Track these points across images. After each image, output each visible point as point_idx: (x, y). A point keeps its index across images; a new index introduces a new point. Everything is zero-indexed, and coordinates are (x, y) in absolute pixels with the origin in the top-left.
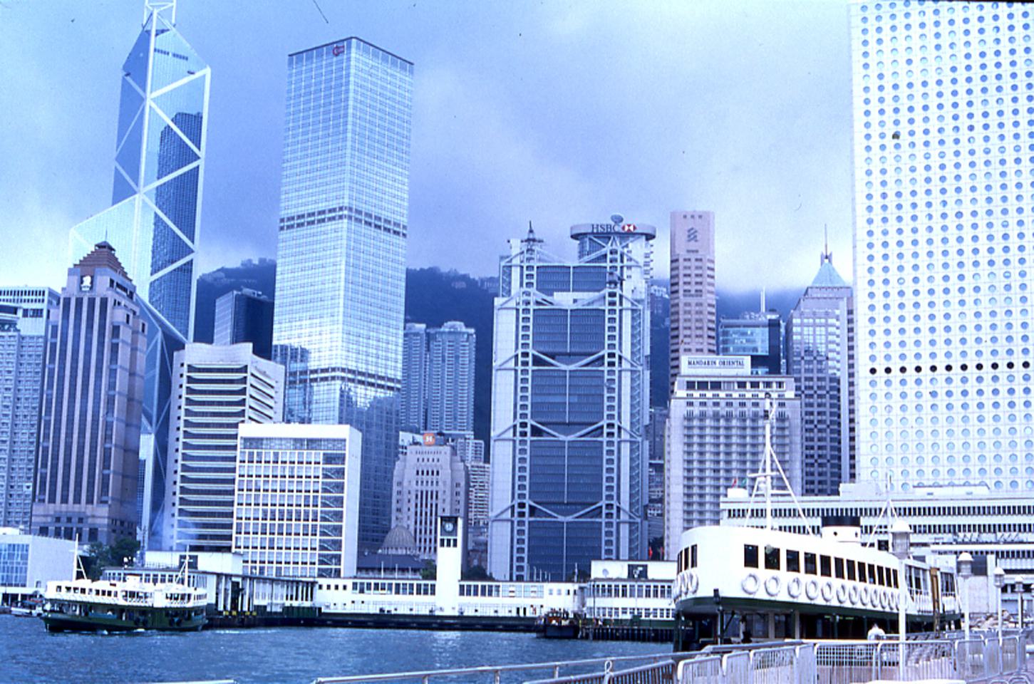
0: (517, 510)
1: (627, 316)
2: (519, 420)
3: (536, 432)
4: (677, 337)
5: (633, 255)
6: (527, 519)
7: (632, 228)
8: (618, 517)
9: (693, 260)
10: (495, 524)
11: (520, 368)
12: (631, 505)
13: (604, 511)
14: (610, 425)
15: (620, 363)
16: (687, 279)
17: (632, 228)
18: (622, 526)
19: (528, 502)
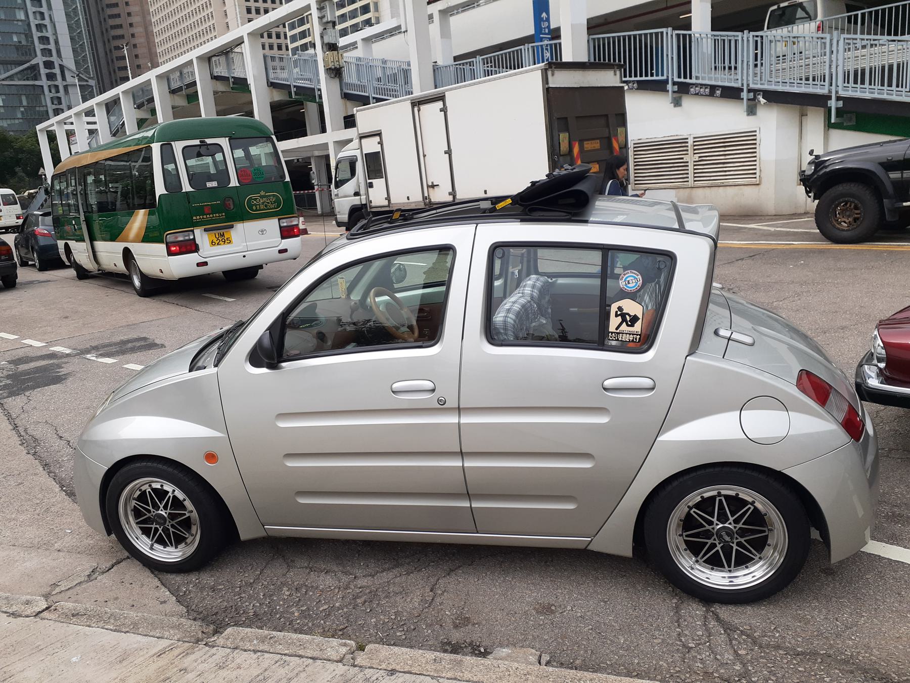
8: (64, 78)
12: (76, 62)
13: (43, 71)
18: (70, 90)
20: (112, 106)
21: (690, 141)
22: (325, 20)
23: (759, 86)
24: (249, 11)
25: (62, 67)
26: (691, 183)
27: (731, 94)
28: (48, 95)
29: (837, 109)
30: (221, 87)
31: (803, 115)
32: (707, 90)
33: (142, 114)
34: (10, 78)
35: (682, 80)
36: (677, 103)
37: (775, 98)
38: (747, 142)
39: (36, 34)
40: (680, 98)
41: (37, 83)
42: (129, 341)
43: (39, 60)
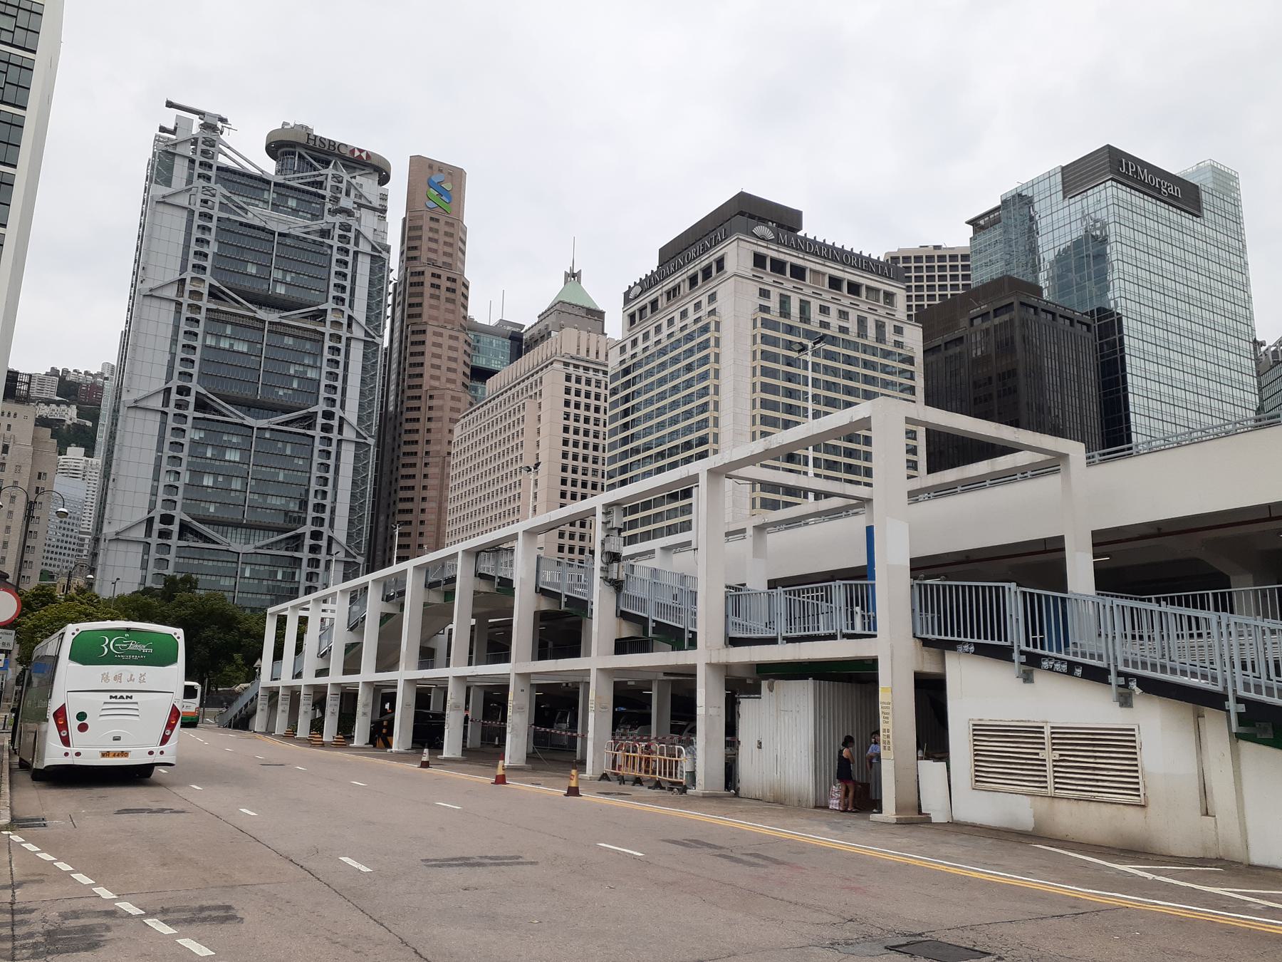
0: (157, 526)
1: (364, 265)
2: (175, 383)
3: (201, 405)
4: (420, 315)
5: (364, 191)
6: (174, 541)
7: (364, 155)
9: (442, 222)
10: (113, 546)
11: (186, 300)
12: (349, 536)
13: (308, 542)
14: (328, 415)
15: (349, 326)
16: (434, 246)
17: (364, 155)
19: (179, 514)
20: (357, 596)
21: (1047, 731)
22: (609, 526)
23: (1130, 670)
24: (563, 495)
25: (330, 539)
26: (1050, 791)
27: (1096, 675)
28: (305, 568)
29: (1239, 714)
30: (484, 587)
31: (1199, 716)
32: (1065, 667)
33: (389, 608)
34: (269, 546)
35: (1031, 649)
36: (1028, 678)
37: (1153, 687)
38: (1122, 743)
39: (312, 501)
40: (1031, 672)
41: (297, 554)
42: (208, 908)
43: (307, 529)
